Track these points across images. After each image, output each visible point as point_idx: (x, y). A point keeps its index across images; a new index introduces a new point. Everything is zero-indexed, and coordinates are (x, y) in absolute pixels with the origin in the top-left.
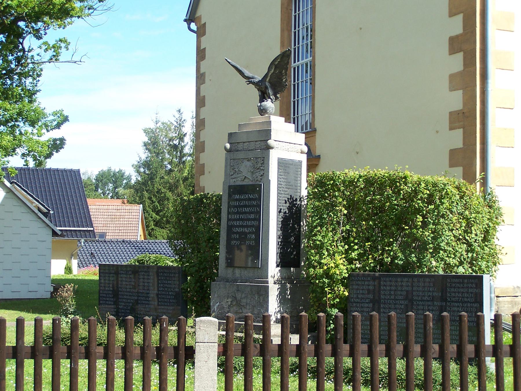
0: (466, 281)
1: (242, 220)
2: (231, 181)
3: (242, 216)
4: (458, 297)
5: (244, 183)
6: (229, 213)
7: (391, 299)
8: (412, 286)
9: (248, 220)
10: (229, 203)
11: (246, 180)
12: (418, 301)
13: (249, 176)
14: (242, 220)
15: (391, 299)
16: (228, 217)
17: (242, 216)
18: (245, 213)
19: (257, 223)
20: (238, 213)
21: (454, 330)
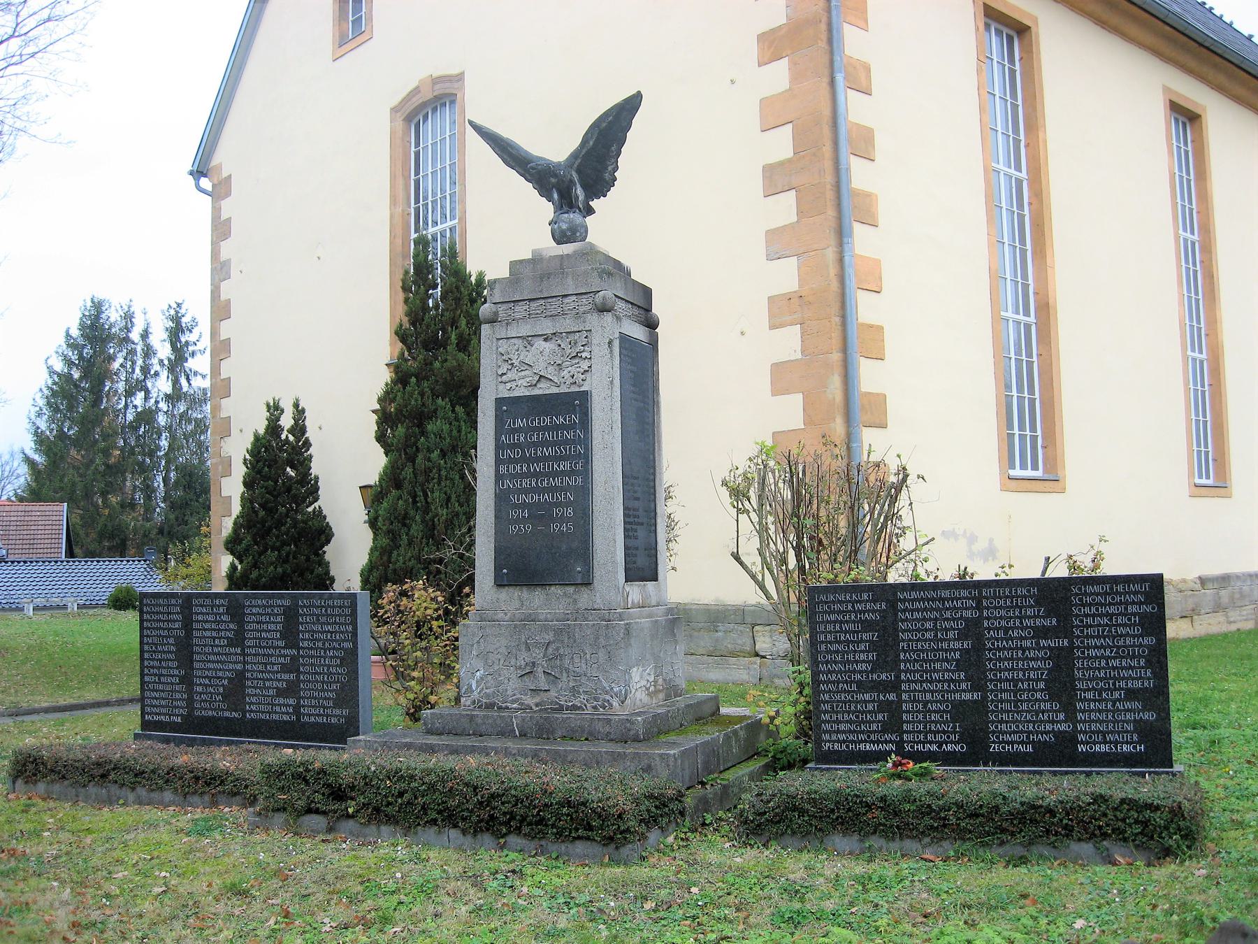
0: (1120, 588)
1: (536, 475)
2: (501, 387)
3: (538, 467)
4: (1100, 625)
5: (536, 392)
6: (498, 462)
7: (926, 640)
8: (979, 607)
9: (555, 474)
10: (497, 439)
11: (542, 385)
12: (997, 640)
13: (550, 372)
14: (536, 475)
15: (926, 640)
16: (497, 471)
17: (538, 467)
18: (544, 459)
19: (580, 480)
20: (523, 459)
21: (1095, 701)
